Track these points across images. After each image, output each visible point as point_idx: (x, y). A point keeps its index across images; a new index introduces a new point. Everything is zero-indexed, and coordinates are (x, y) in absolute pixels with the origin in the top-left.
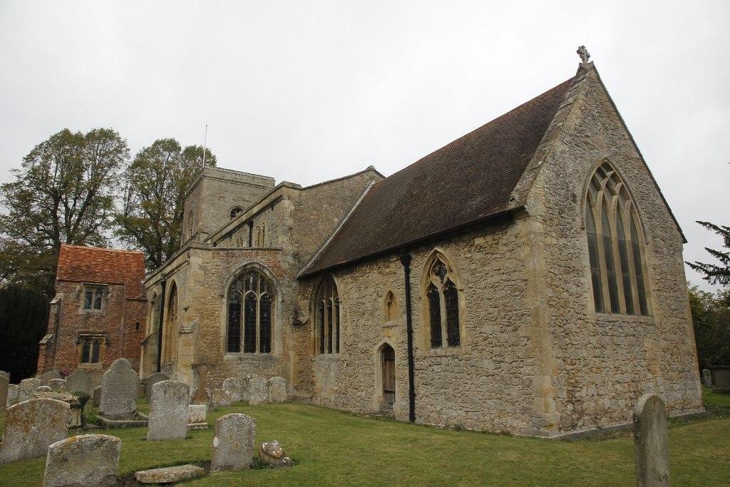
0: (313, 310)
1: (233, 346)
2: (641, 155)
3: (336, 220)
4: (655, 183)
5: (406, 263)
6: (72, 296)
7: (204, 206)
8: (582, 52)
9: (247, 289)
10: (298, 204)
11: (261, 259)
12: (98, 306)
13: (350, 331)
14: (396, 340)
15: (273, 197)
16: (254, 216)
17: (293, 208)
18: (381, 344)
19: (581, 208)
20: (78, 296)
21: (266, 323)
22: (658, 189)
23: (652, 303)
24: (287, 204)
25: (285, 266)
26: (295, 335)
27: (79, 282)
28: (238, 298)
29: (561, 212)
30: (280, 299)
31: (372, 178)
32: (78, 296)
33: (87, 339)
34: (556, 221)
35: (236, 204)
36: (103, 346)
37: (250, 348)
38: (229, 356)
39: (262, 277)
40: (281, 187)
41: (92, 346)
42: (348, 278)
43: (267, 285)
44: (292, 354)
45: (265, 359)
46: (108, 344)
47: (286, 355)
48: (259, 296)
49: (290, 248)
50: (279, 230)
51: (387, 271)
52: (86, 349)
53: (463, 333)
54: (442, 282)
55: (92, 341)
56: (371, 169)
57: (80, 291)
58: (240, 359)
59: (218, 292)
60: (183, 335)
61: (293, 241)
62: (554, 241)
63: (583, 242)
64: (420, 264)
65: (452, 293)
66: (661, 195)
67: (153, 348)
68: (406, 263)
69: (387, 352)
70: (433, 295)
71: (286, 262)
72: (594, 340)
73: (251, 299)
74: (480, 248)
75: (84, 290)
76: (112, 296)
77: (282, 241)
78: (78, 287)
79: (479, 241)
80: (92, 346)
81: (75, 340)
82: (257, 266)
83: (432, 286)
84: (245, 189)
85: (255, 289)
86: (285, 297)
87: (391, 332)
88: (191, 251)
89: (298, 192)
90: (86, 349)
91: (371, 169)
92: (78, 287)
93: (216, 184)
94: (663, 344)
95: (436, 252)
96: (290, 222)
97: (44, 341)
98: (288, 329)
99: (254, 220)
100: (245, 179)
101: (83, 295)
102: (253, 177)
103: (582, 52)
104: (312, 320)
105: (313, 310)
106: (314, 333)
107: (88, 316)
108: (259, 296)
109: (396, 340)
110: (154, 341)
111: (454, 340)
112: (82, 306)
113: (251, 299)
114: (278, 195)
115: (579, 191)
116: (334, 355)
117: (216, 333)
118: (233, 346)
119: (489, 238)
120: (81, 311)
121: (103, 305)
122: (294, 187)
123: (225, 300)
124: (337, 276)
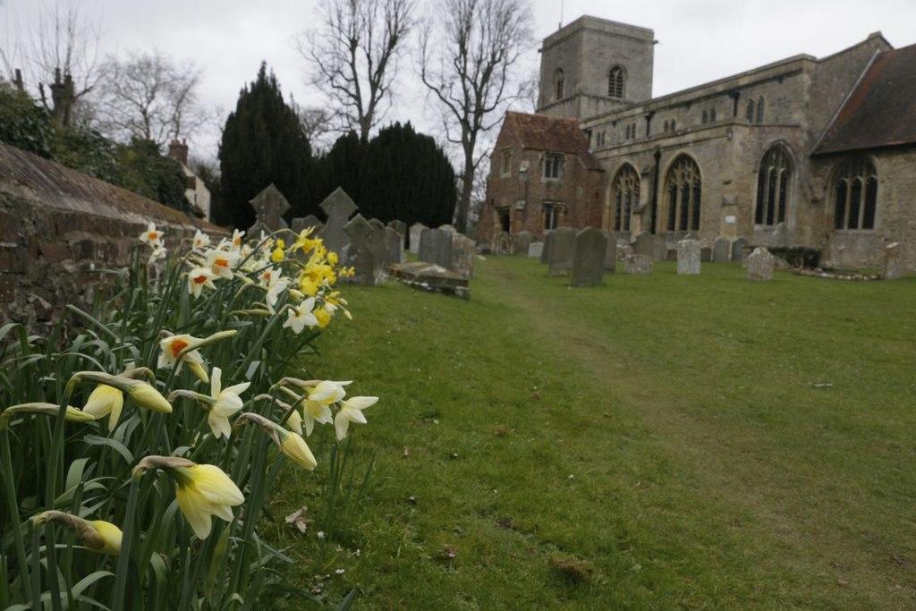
0: (829, 186)
1: (759, 221)
3: (842, 95)
6: (536, 163)
7: (585, 64)
10: (814, 78)
11: (786, 135)
12: (555, 175)
13: (895, 208)
15: (783, 69)
17: (810, 82)
20: (540, 165)
24: (805, 79)
26: (813, 211)
27: (541, 150)
30: (797, 177)
31: (877, 46)
32: (540, 165)
33: (549, 207)
35: (614, 61)
36: (561, 215)
38: (757, 227)
39: (783, 154)
40: (802, 59)
41: (552, 214)
42: (899, 160)
44: (808, 229)
46: (565, 212)
49: (805, 125)
50: (793, 106)
52: (548, 216)
55: (553, 210)
56: (877, 39)
57: (542, 160)
59: (752, 167)
60: (726, 207)
61: (810, 118)
67: (647, 218)
71: (802, 138)
73: (774, 172)
75: (545, 158)
76: (567, 166)
77: (798, 117)
78: (540, 155)
80: (552, 214)
82: (782, 143)
84: (624, 43)
88: (734, 128)
89: (814, 65)
90: (548, 216)
91: (877, 39)
92: (540, 155)
93: (595, 37)
96: (807, 97)
98: (804, 205)
99: (741, 92)
100: (624, 32)
101: (544, 163)
102: (632, 28)
104: (827, 197)
105: (829, 186)
106: (829, 209)
107: (549, 185)
110: (648, 211)
112: (544, 174)
113: (774, 172)
116: (860, 230)
117: (750, 209)
118: (759, 221)
120: (544, 180)
121: (560, 173)
122: (813, 60)
123: (757, 175)
124: (877, 156)
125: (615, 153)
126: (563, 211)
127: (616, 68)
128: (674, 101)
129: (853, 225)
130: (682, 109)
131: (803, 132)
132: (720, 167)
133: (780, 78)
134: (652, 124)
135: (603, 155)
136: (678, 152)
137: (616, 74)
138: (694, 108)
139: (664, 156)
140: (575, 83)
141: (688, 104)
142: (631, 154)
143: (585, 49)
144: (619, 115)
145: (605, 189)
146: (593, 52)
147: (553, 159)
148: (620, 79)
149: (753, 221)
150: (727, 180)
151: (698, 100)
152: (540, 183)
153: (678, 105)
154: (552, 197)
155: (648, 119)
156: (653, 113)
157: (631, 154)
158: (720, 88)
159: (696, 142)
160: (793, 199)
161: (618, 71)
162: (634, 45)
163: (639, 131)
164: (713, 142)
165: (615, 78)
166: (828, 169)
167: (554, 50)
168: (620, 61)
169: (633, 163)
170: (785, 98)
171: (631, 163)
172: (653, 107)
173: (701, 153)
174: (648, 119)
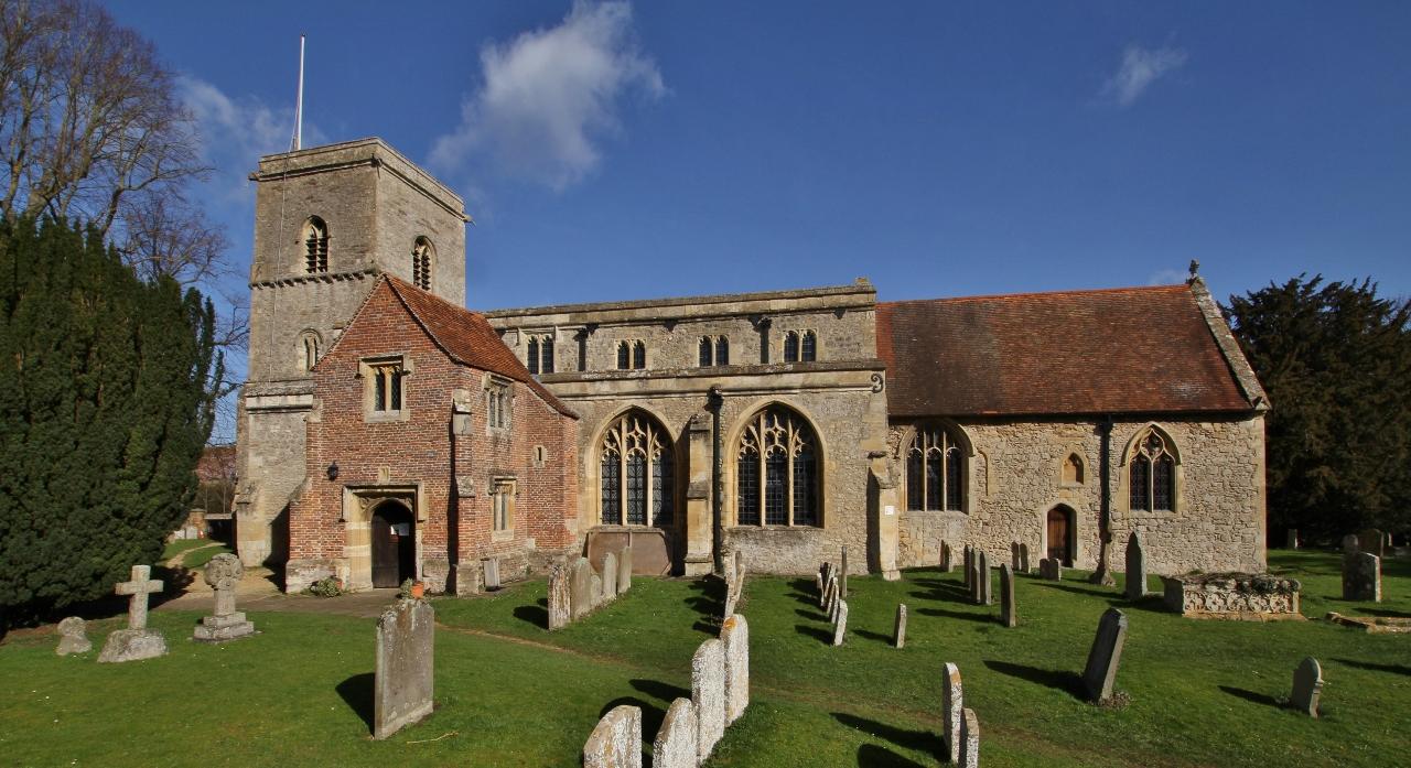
5: (1104, 432)
7: (381, 223)
14: (1082, 501)
16: (775, 313)
18: (1052, 504)
42: (991, 430)
51: (1069, 432)
53: (1180, 500)
54: (1151, 454)
64: (1129, 438)
65: (1168, 466)
68: (1104, 432)
69: (1063, 516)
70: (1140, 466)
74: (1207, 433)
76: (516, 405)
79: (1205, 425)
80: (499, 498)
81: (487, 488)
83: (1140, 456)
87: (1070, 493)
93: (395, 182)
95: (1153, 426)
105: (902, 458)
107: (496, 440)
109: (1082, 501)
111: (1168, 502)
114: (862, 302)
119: (1218, 426)
121: (507, 419)
124: (964, 424)
125: (605, 387)
126: (514, 492)
127: (421, 241)
128: (641, 314)
129: (936, 504)
130: (657, 329)
132: (862, 430)
133: (839, 311)
134: (590, 341)
135: (574, 388)
136: (766, 400)
137: (421, 250)
138: (680, 329)
139: (728, 404)
140: (363, 250)
141: (670, 323)
142: (650, 394)
143: (381, 197)
144: (513, 321)
145: (582, 450)
146: (392, 206)
148: (425, 259)
150: (875, 450)
151: (693, 319)
152: (486, 439)
153: (649, 322)
154: (501, 467)
155: (581, 337)
156: (592, 327)
157: (650, 394)
158: (735, 308)
159: (804, 387)
161: (423, 248)
162: (444, 214)
163: (561, 351)
164: (841, 393)
165: (420, 257)
166: (908, 433)
167: (297, 182)
168: (426, 232)
169: (657, 408)
170: (848, 339)
171: (649, 409)
172: (594, 317)
173: (819, 407)
174: (581, 337)
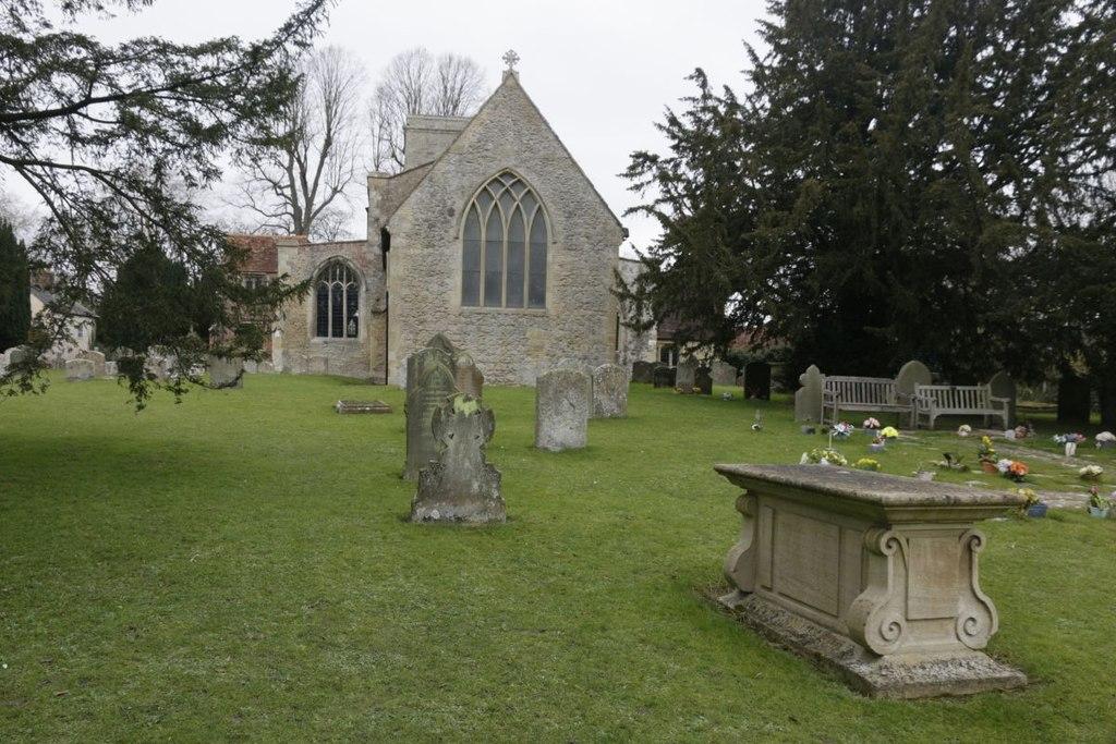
1: (321, 330)
2: (569, 154)
4: (587, 180)
8: (511, 58)
9: (334, 279)
17: (380, 198)
19: (458, 224)
21: (353, 308)
22: (592, 186)
23: (550, 297)
25: (371, 257)
28: (325, 288)
29: (431, 226)
34: (424, 235)
37: (338, 333)
43: (351, 276)
45: (350, 343)
47: (368, 339)
48: (345, 286)
58: (326, 343)
62: (417, 252)
63: (457, 250)
66: (596, 192)
72: (454, 328)
73: (337, 289)
82: (341, 259)
85: (341, 280)
86: (371, 287)
93: (423, 136)
94: (558, 333)
97: (210, 329)
103: (511, 58)
108: (345, 286)
113: (337, 289)
115: (459, 205)
118: (321, 330)
131: (372, 246)
147: (254, 280)
149: (309, 330)
160: (362, 313)
